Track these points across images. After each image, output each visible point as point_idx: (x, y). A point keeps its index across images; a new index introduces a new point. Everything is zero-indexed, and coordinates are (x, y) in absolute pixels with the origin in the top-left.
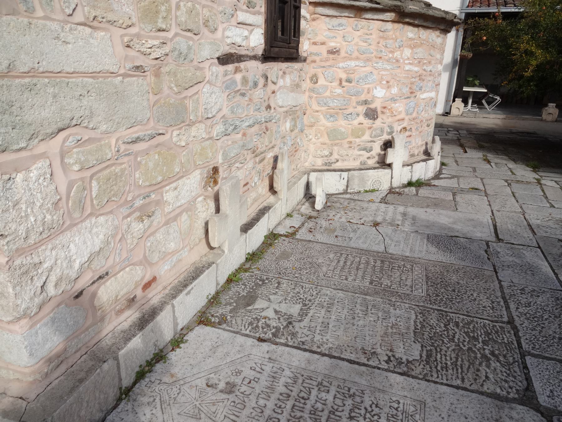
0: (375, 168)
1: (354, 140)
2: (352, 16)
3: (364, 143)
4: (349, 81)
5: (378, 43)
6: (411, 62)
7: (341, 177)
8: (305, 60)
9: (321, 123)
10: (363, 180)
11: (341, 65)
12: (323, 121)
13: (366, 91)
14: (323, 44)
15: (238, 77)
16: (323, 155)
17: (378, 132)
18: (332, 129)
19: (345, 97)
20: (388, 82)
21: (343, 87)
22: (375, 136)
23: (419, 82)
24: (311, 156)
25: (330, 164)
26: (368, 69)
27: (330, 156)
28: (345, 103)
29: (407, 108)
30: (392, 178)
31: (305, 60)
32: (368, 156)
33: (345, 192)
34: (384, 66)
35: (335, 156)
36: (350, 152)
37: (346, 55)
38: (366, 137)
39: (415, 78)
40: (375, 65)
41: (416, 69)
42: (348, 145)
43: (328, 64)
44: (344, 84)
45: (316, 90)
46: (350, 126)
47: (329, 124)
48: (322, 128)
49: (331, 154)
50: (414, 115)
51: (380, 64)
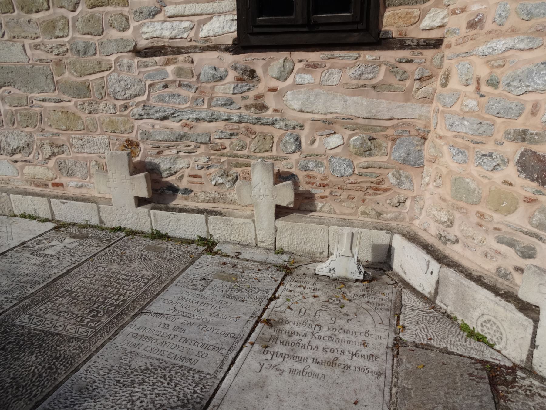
1: (489, 213)
3: (509, 230)
4: (493, 83)
7: (428, 265)
8: (437, 44)
9: (443, 160)
11: (482, 49)
12: (447, 158)
13: (529, 108)
15: (170, 69)
16: (439, 218)
18: (457, 176)
19: (483, 118)
21: (482, 96)
24: (424, 212)
27: (448, 226)
28: (481, 131)
32: (518, 265)
36: (480, 235)
37: (494, 27)
38: (519, 218)
44: (485, 89)
45: (442, 98)
46: (485, 181)
47: (454, 166)
48: (444, 171)
49: (451, 224)
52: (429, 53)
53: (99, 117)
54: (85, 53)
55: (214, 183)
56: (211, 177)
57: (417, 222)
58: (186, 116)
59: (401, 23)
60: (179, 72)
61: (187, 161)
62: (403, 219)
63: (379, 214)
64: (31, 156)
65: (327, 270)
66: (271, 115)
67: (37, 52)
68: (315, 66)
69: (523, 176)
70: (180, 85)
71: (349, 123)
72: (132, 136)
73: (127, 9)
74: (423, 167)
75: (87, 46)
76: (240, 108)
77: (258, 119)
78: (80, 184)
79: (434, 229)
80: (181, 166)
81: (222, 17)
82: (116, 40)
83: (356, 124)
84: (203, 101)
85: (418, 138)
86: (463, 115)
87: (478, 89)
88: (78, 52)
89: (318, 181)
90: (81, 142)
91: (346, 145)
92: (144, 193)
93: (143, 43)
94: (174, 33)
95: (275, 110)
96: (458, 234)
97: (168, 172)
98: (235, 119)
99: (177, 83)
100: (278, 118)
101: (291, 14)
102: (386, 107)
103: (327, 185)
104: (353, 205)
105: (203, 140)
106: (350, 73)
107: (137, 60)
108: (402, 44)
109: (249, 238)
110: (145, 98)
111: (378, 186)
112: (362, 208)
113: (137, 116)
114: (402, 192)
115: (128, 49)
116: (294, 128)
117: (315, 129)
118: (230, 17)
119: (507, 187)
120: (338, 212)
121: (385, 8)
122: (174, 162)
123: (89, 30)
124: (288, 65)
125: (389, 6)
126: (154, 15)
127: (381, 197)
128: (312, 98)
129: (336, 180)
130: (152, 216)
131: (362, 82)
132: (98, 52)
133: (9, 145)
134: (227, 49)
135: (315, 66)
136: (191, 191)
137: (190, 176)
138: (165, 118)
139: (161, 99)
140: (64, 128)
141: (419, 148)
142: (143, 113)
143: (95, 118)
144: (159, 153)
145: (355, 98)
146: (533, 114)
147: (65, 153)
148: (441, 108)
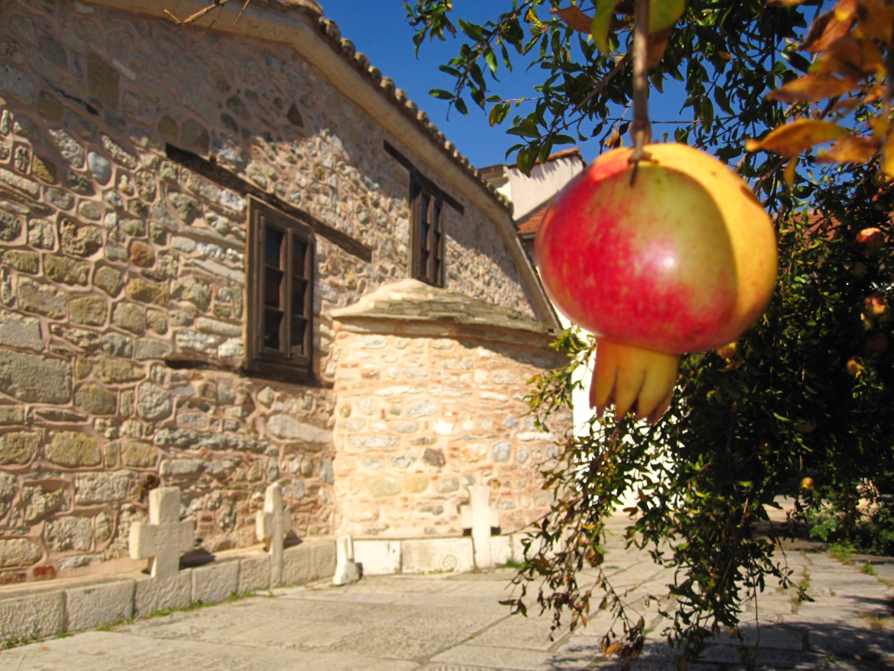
4: (396, 412)
7: (389, 547)
10: (425, 555)
11: (382, 392)
13: (422, 426)
14: (355, 366)
17: (449, 484)
20: (455, 414)
22: (444, 491)
24: (344, 521)
25: (376, 531)
29: (495, 451)
30: (474, 552)
31: (330, 386)
33: (399, 571)
35: (383, 520)
36: (406, 514)
38: (430, 491)
39: (502, 409)
41: (502, 397)
42: (399, 504)
43: (364, 391)
44: (389, 416)
49: (377, 516)
50: (510, 462)
61: (201, 499)
86: (374, 435)
87: (383, 417)
96: (388, 521)
98: (241, 445)
115: (164, 355)
119: (419, 475)
134: (235, 372)
146: (426, 428)
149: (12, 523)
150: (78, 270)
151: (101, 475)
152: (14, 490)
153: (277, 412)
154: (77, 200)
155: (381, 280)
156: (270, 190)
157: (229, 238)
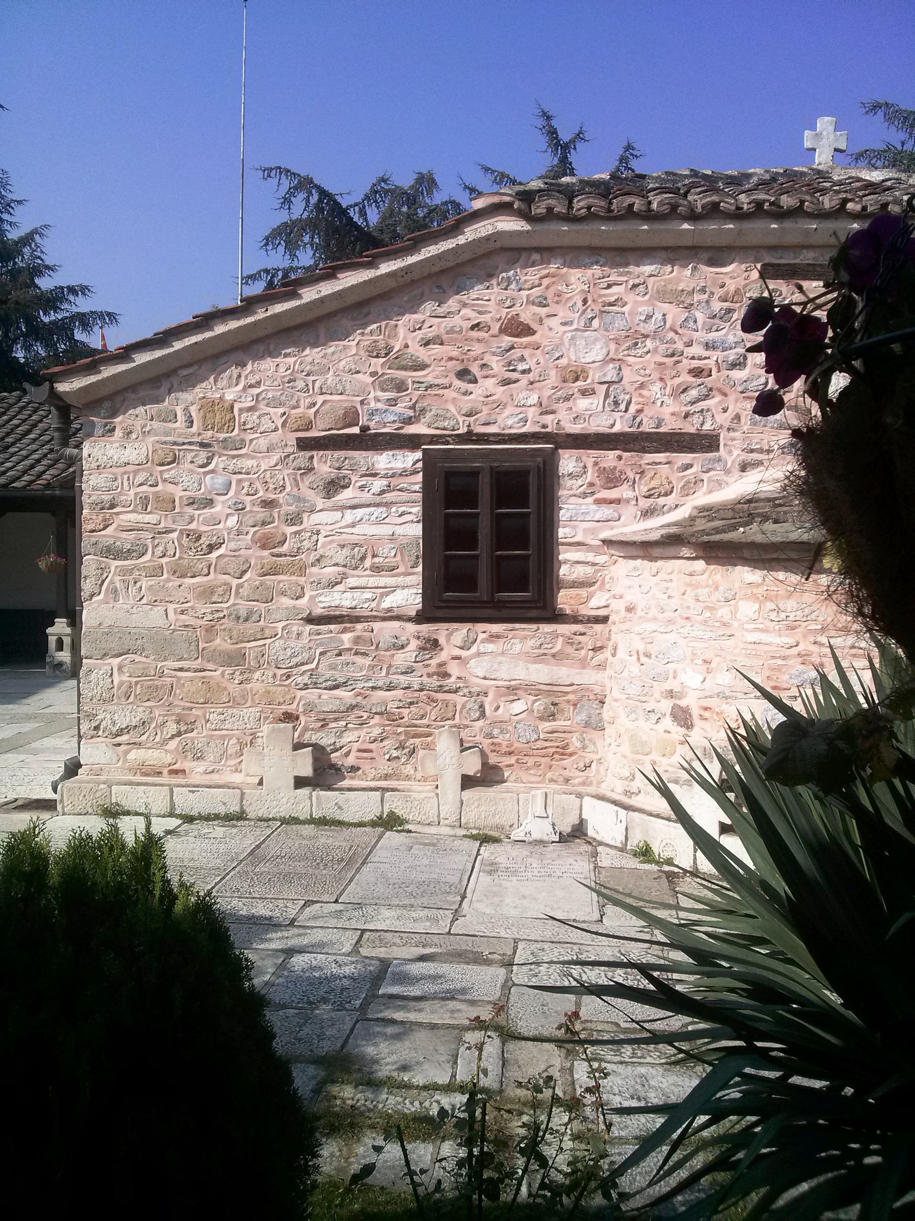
0: (669, 819)
2: (642, 554)
4: (648, 656)
5: (684, 594)
6: (761, 626)
8: (604, 620)
13: (671, 674)
15: (347, 637)
16: (622, 775)
23: (801, 667)
26: (672, 637)
28: (644, 692)
34: (696, 633)
37: (643, 614)
39: (784, 658)
40: (681, 630)
43: (626, 626)
46: (653, 733)
51: (688, 628)
52: (598, 627)
53: (251, 688)
54: (246, 620)
55: (387, 757)
56: (385, 750)
57: (603, 785)
58: (360, 685)
59: (572, 602)
60: (357, 640)
61: (356, 733)
62: (591, 784)
63: (567, 780)
64: (144, 737)
65: (523, 834)
66: (455, 683)
67: (183, 617)
68: (498, 637)
69: (675, 724)
70: (356, 653)
71: (533, 689)
72: (292, 708)
73: (303, 579)
74: (604, 729)
75: (250, 614)
76: (421, 676)
77: (440, 686)
78: (211, 769)
79: (620, 786)
80: (348, 740)
81: (406, 590)
82: (287, 608)
83: (539, 690)
84: (381, 669)
85: (597, 702)
87: (639, 659)
88: (238, 618)
89: (504, 749)
90: (222, 717)
91: (530, 711)
92: (307, 771)
93: (318, 611)
94: (354, 604)
95: (459, 678)
97: (332, 747)
98: (416, 687)
99: (353, 652)
100: (462, 685)
101: (475, 591)
102: (564, 674)
103: (513, 752)
104: (540, 773)
105: (378, 710)
106: (531, 643)
107: (309, 627)
108: (575, 619)
109: (431, 815)
110: (313, 666)
111: (564, 751)
112: (549, 775)
113: (300, 686)
114: (588, 755)
116: (478, 695)
117: (499, 696)
118: (415, 591)
120: (524, 781)
121: (559, 589)
122: (340, 736)
123: (256, 598)
124: (472, 636)
125: (562, 588)
126: (333, 586)
127: (568, 762)
128: (496, 666)
129: (523, 745)
130: (314, 799)
131: (542, 651)
132: (262, 619)
133: (114, 723)
134: (410, 620)
135: (498, 637)
136: (359, 769)
137: (359, 751)
138: (336, 687)
139: (333, 667)
140: (202, 701)
141: (598, 711)
142: (309, 682)
143: (246, 689)
144: (323, 726)
145: (536, 666)
147: (196, 731)
148: (614, 675)
149: (152, 739)
150: (201, 566)
151: (230, 711)
152: (152, 719)
153: (479, 654)
154: (196, 517)
155: (744, 467)
156: (463, 430)
157: (389, 497)
